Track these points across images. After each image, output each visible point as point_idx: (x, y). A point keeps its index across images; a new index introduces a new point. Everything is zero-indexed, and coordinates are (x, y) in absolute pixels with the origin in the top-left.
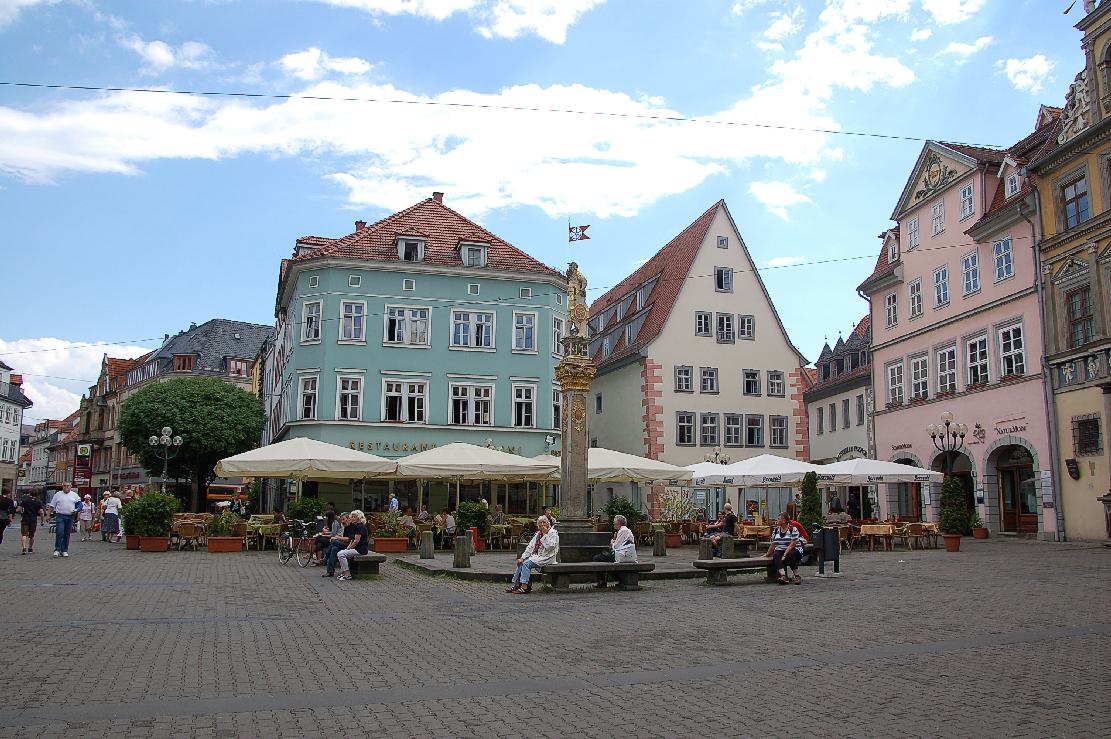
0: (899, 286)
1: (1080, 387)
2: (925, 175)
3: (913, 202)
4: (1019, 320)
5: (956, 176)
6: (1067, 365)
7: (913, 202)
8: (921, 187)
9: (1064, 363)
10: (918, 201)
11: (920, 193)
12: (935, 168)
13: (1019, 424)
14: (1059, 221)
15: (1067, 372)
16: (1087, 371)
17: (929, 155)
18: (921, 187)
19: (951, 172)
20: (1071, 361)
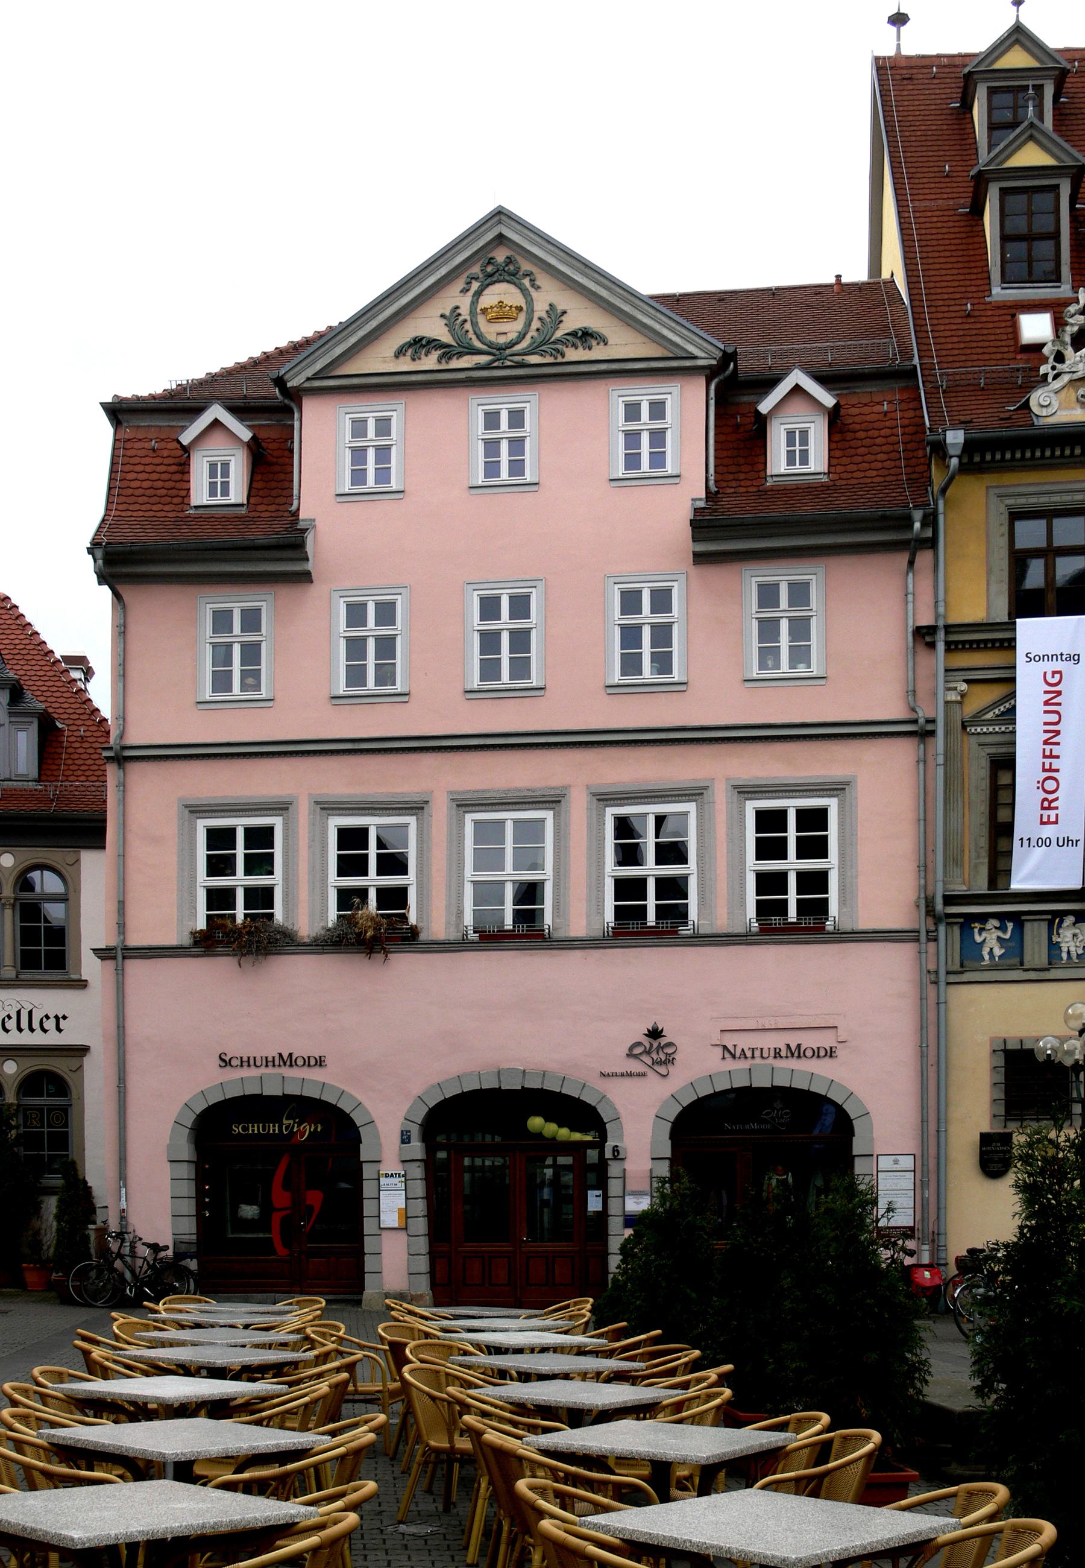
0: (285, 592)
1: (1032, 975)
2: (456, 298)
5: (598, 352)
6: (993, 923)
8: (429, 324)
9: (983, 918)
10: (405, 365)
11: (420, 345)
12: (501, 293)
13: (810, 1041)
15: (991, 940)
16: (1054, 947)
17: (498, 250)
19: (585, 336)
20: (1002, 917)
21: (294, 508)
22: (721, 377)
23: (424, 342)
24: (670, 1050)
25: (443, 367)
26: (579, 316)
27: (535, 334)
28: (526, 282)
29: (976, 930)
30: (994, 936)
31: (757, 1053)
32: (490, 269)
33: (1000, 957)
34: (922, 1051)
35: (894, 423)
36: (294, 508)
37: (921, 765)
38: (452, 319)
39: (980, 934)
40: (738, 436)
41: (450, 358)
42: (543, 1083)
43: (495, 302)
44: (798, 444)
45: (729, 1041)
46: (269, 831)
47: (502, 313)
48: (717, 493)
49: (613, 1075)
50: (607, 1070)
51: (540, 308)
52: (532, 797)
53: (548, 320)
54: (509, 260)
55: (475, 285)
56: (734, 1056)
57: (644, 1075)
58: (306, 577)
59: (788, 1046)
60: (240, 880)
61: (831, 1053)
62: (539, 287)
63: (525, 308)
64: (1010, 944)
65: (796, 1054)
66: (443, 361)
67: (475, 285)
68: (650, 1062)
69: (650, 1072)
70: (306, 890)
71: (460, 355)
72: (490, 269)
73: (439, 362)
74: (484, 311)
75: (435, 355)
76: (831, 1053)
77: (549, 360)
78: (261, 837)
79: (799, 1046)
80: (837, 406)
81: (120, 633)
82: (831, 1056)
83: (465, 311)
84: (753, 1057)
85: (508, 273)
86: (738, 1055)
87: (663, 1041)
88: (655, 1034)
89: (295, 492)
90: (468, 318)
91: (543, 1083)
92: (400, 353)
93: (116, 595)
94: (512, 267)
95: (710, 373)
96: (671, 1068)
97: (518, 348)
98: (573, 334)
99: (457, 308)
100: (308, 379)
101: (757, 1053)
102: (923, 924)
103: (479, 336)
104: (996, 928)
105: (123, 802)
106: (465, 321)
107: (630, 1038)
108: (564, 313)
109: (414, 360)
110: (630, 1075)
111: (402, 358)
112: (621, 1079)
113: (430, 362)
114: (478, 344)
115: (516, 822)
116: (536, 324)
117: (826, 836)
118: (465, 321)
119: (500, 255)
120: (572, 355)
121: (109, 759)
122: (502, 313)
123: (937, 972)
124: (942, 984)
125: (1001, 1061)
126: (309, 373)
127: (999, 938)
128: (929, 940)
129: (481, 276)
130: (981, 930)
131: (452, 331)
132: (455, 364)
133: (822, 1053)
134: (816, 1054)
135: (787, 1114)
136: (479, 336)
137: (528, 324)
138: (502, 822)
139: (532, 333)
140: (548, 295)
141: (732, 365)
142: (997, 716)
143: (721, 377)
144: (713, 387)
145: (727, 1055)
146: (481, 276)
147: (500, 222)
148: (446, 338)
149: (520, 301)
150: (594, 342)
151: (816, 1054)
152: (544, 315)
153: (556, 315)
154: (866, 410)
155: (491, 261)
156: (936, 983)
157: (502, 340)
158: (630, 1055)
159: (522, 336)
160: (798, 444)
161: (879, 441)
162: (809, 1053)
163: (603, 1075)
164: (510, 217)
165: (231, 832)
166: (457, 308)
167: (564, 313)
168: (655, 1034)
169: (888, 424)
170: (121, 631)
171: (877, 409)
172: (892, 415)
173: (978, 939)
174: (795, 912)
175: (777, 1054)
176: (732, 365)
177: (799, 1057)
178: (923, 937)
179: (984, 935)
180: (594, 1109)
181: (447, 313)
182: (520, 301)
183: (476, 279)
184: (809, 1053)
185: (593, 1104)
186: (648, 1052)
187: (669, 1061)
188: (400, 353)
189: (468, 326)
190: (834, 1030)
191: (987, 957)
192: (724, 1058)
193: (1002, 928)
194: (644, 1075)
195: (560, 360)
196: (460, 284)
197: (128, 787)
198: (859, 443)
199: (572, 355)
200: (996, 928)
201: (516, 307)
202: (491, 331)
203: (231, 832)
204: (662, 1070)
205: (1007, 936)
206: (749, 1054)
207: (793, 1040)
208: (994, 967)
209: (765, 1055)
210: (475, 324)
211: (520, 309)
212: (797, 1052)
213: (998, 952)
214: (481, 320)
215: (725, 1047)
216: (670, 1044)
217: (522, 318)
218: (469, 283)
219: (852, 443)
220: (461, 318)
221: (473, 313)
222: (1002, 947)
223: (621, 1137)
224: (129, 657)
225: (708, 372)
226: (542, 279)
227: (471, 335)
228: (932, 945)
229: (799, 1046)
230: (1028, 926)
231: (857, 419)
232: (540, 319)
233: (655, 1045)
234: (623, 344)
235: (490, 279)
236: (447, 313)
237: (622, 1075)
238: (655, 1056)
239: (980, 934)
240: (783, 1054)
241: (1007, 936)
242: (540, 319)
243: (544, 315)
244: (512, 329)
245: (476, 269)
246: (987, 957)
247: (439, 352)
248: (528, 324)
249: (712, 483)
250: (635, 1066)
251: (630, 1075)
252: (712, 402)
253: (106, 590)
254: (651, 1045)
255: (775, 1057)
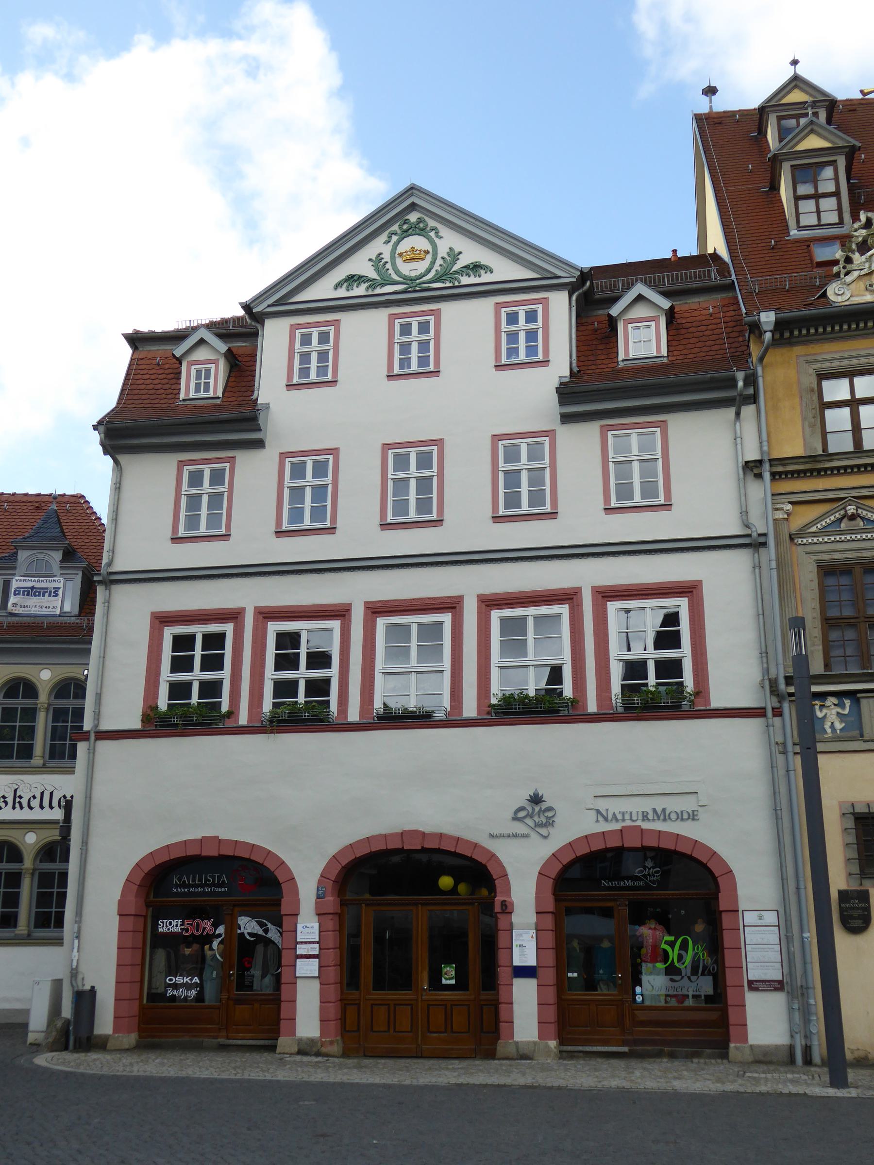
2: (379, 246)
3: (324, 289)
4: (690, 590)
5: (486, 278)
7: (324, 289)
9: (823, 696)
10: (342, 293)
11: (352, 280)
13: (674, 805)
14: (812, 426)
18: (360, 264)
19: (476, 268)
21: (254, 397)
22: (581, 291)
23: (355, 278)
24: (550, 814)
25: (370, 293)
26: (471, 253)
27: (439, 269)
28: (432, 234)
29: (817, 707)
30: (834, 712)
31: (627, 817)
32: (405, 227)
33: (841, 730)
34: (776, 814)
35: (718, 321)
36: (254, 397)
37: (757, 570)
38: (378, 262)
39: (821, 711)
40: (596, 332)
41: (374, 288)
42: (440, 844)
43: (408, 249)
44: (642, 339)
45: (602, 805)
46: (221, 636)
47: (412, 257)
48: (579, 372)
49: (501, 836)
50: (495, 832)
51: (443, 251)
52: (432, 604)
53: (448, 258)
54: (420, 220)
55: (395, 238)
56: (606, 819)
57: (527, 836)
58: (259, 444)
59: (654, 810)
60: (197, 675)
61: (693, 816)
62: (442, 237)
63: (431, 251)
64: (849, 719)
65: (662, 817)
66: (370, 290)
67: (395, 238)
68: (532, 825)
69: (533, 835)
70: (248, 680)
71: (382, 285)
72: (405, 227)
73: (367, 289)
74: (400, 255)
75: (364, 286)
76: (693, 816)
77: (448, 284)
78: (214, 641)
79: (664, 810)
80: (672, 308)
81: (116, 488)
82: (693, 819)
83: (386, 257)
84: (623, 820)
85: (419, 229)
86: (610, 818)
87: (544, 806)
88: (536, 799)
89: (256, 385)
90: (389, 261)
91: (440, 844)
92: (338, 286)
93: (116, 462)
94: (421, 225)
95: (572, 288)
96: (550, 829)
97: (425, 279)
98: (467, 267)
99: (381, 254)
100: (269, 306)
101: (627, 817)
102: (770, 703)
103: (397, 272)
104: (835, 705)
105: (107, 614)
106: (387, 262)
107: (515, 800)
108: (460, 253)
109: (348, 290)
110: (515, 836)
111: (339, 290)
112: (509, 841)
113: (361, 290)
114: (395, 277)
115: (420, 625)
116: (439, 261)
117: (679, 631)
118: (387, 262)
119: (413, 217)
120: (465, 280)
121: (100, 582)
122: (414, 257)
123: (784, 744)
124: (790, 755)
125: (851, 823)
126: (271, 301)
127: (838, 713)
128: (774, 715)
129: (399, 232)
130: (822, 707)
131: (377, 269)
132: (378, 291)
133: (685, 816)
134: (680, 817)
135: (657, 872)
136: (397, 272)
137: (433, 262)
138: (408, 626)
139: (437, 267)
140: (449, 240)
141: (588, 283)
142: (825, 527)
143: (581, 291)
144: (574, 298)
145: (600, 818)
146: (399, 232)
147: (412, 195)
148: (372, 274)
149: (427, 246)
150: (483, 272)
151: (680, 817)
152: (446, 256)
153: (454, 255)
154: (697, 313)
155: (406, 222)
156: (784, 752)
157: (413, 274)
158: (515, 819)
159: (429, 271)
160: (642, 339)
161: (708, 333)
162: (674, 816)
163: (491, 836)
164: (419, 191)
165: (191, 638)
166: (381, 254)
167: (460, 253)
168: (536, 799)
169: (714, 321)
170: (118, 487)
171: (705, 312)
172: (717, 316)
173: (820, 714)
174: (659, 694)
175: (645, 817)
176: (588, 283)
177: (665, 820)
178: (769, 713)
179: (825, 711)
180: (485, 866)
181: (374, 258)
182: (429, 248)
183: (396, 234)
184: (674, 816)
185: (484, 862)
186: (530, 816)
187: (549, 823)
188: (338, 286)
189: (388, 266)
190: (692, 798)
191: (829, 730)
192: (598, 821)
193: (841, 705)
194: (527, 836)
195: (457, 284)
196: (384, 237)
197: (112, 602)
198: (692, 335)
199: (465, 280)
200: (835, 705)
201: (425, 251)
202: (407, 269)
203: (191, 638)
204: (544, 831)
205: (846, 712)
206: (620, 817)
207: (659, 804)
208: (836, 739)
209: (634, 818)
210: (394, 264)
211: (427, 252)
212: (664, 815)
213: (839, 726)
214: (399, 261)
215: (598, 812)
216: (550, 809)
217: (429, 258)
218: (390, 237)
219: (686, 336)
220: (383, 261)
221: (393, 257)
222: (841, 722)
223: (508, 892)
224: (121, 502)
225: (570, 287)
226: (444, 231)
227: (391, 271)
228: (777, 720)
229: (664, 810)
230: (864, 702)
231: (689, 320)
232: (442, 258)
233: (537, 809)
234: (505, 270)
235: (405, 234)
236: (374, 258)
237: (509, 836)
238: (536, 819)
239: (821, 711)
240: (650, 817)
241: (846, 712)
242: (442, 258)
243: (446, 256)
244: (420, 267)
245: (395, 227)
246: (829, 730)
247: (367, 284)
248: (433, 262)
249: (574, 365)
250: (519, 828)
251: (515, 836)
252: (574, 309)
253: (109, 460)
254: (533, 809)
255: (643, 820)
